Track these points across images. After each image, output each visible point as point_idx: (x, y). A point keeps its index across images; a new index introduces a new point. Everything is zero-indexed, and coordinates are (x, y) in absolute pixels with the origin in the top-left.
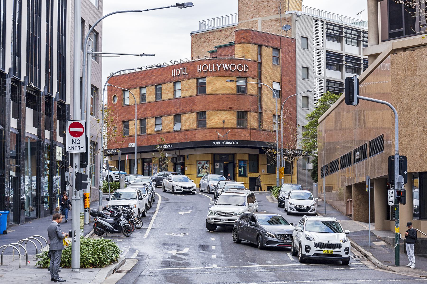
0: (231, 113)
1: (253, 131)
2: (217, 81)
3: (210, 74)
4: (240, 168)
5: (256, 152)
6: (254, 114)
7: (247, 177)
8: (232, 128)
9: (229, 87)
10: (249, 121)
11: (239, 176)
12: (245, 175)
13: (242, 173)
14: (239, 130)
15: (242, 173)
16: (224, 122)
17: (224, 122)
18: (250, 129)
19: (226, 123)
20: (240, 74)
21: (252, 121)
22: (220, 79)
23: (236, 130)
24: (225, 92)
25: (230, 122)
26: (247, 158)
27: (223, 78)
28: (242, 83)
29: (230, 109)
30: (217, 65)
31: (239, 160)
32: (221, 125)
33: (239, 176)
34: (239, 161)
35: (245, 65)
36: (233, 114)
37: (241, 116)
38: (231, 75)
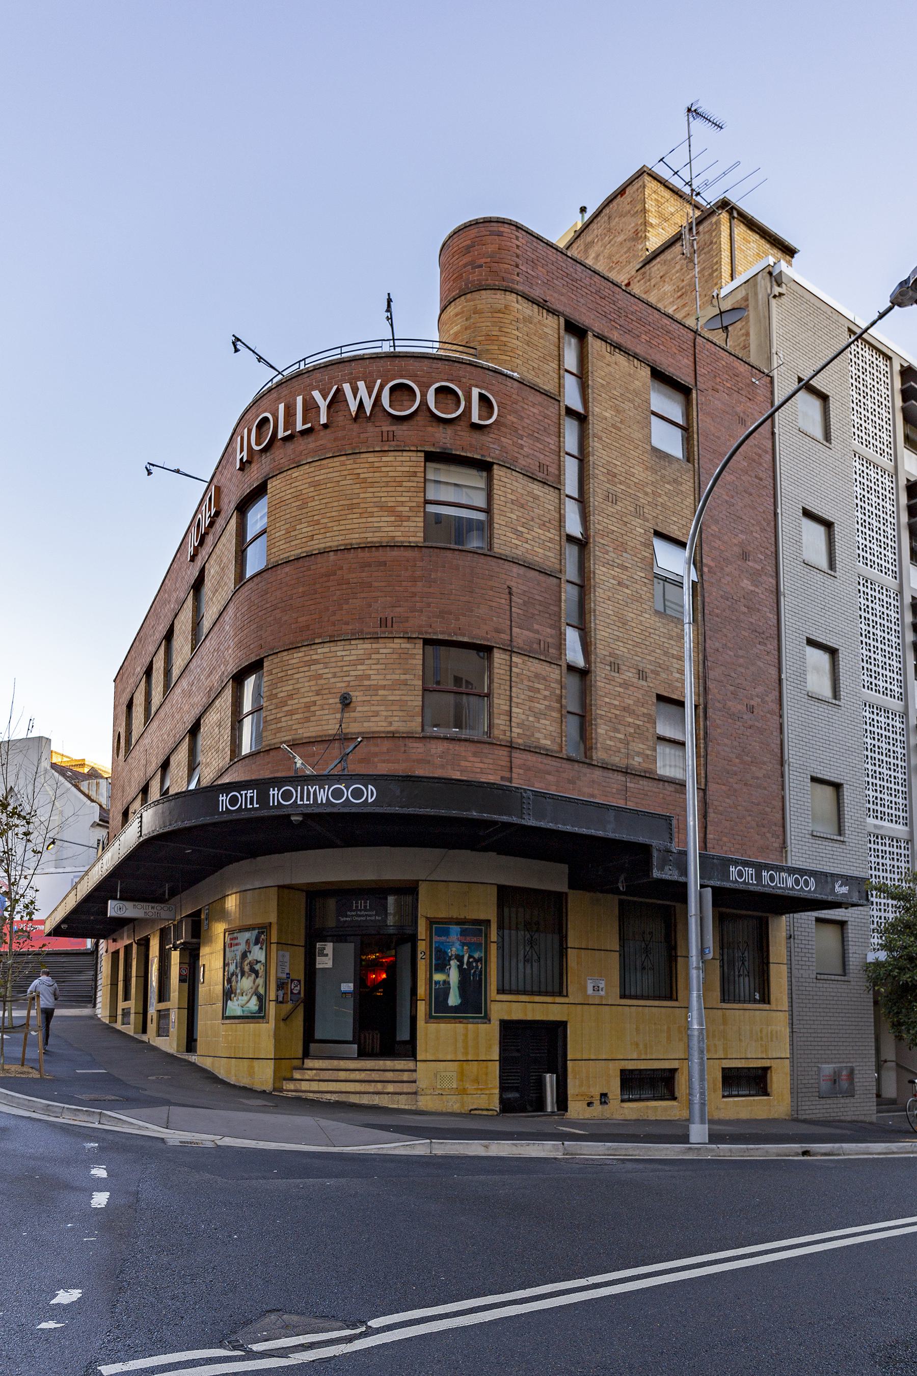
0: (386, 649)
1: (531, 759)
2: (316, 485)
3: (280, 454)
4: (442, 966)
5: (551, 877)
6: (536, 667)
7: (487, 1019)
8: (393, 736)
9: (383, 507)
10: (500, 703)
11: (430, 1018)
12: (473, 1005)
13: (454, 999)
14: (437, 748)
15: (454, 999)
16: (346, 702)
17: (346, 702)
18: (511, 746)
19: (360, 710)
20: (444, 439)
21: (525, 702)
22: (333, 470)
23: (417, 749)
24: (355, 538)
25: (384, 702)
26: (488, 911)
27: (349, 462)
28: (457, 492)
29: (385, 629)
30: (316, 394)
31: (431, 922)
32: (328, 722)
33: (430, 1018)
34: (438, 926)
35: (475, 392)
36: (404, 656)
37: (457, 668)
38: (391, 445)
